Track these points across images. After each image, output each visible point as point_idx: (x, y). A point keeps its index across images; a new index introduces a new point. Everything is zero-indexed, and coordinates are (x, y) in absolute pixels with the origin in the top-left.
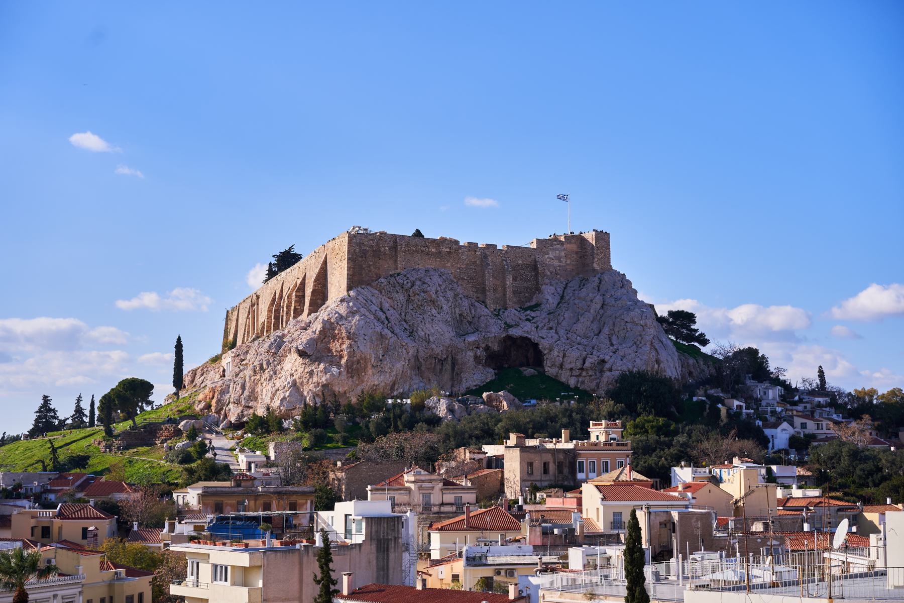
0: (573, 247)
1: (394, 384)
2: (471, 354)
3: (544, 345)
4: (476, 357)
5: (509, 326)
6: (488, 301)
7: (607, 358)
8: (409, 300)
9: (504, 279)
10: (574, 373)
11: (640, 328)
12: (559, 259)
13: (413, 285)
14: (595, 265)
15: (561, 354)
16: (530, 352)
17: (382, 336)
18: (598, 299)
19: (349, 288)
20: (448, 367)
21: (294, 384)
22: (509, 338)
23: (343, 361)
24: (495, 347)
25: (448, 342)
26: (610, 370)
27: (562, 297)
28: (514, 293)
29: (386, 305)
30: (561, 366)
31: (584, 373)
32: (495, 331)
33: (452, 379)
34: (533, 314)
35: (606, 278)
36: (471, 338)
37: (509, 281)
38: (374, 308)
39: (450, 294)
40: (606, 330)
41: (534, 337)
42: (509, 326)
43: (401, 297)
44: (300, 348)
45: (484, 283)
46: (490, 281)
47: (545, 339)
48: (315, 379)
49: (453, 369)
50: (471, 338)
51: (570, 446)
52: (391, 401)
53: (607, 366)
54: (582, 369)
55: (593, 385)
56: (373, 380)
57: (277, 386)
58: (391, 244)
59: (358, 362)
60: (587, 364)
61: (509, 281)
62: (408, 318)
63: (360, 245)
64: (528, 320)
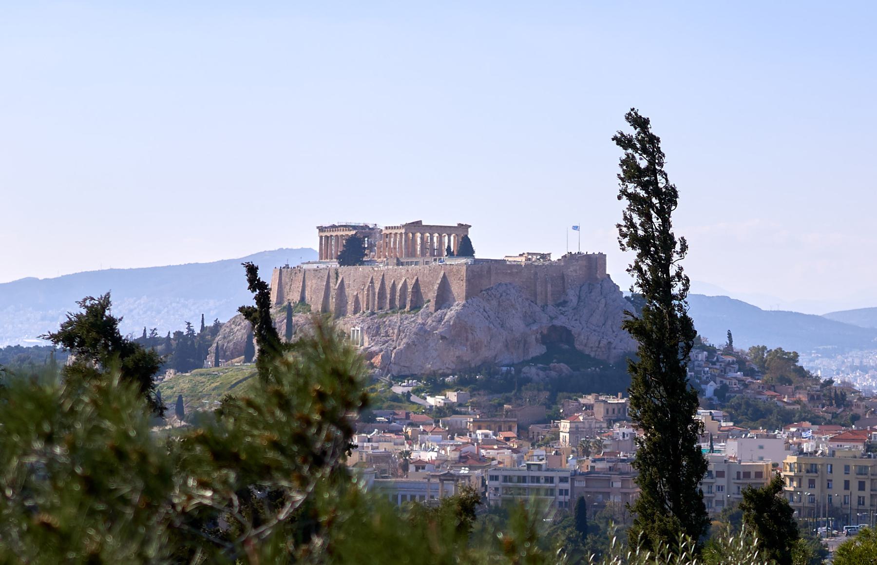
0: (584, 263)
1: (496, 355)
2: (534, 337)
3: (574, 331)
4: (536, 339)
5: (552, 318)
7: (612, 341)
8: (499, 305)
9: (546, 287)
12: (575, 271)
16: (566, 335)
17: (489, 329)
18: (603, 301)
19: (467, 298)
20: (522, 345)
22: (553, 326)
24: (545, 332)
27: (579, 297)
29: (487, 309)
30: (586, 345)
32: (545, 322)
34: (564, 309)
35: (605, 285)
36: (534, 328)
37: (549, 288)
38: (482, 310)
39: (520, 299)
40: (609, 323)
43: (494, 303)
46: (539, 289)
47: (575, 328)
50: (534, 328)
51: (623, 401)
53: (613, 346)
56: (486, 353)
60: (601, 345)
61: (549, 288)
62: (500, 315)
64: (562, 314)
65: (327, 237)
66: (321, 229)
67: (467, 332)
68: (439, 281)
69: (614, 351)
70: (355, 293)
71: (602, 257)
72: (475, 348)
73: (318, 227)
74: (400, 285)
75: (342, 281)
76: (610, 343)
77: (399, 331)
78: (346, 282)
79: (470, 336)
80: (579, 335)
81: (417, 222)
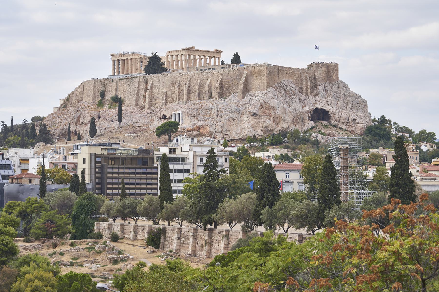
1: (289, 127)
2: (307, 115)
6: (304, 93)
7: (356, 118)
10: (345, 124)
11: (363, 106)
13: (287, 87)
14: (334, 77)
15: (339, 116)
21: (251, 126)
22: (317, 109)
23: (272, 118)
25: (301, 111)
26: (358, 123)
28: (311, 89)
30: (339, 121)
31: (348, 124)
33: (302, 125)
34: (318, 99)
41: (327, 108)
42: (314, 104)
43: (283, 92)
44: (255, 112)
45: (302, 85)
46: (304, 85)
47: (330, 109)
48: (261, 125)
49: (302, 121)
50: (307, 109)
52: (302, 134)
53: (357, 121)
54: (347, 122)
55: (353, 129)
57: (243, 126)
58: (277, 70)
59: (277, 118)
60: (350, 121)
63: (270, 71)
65: (119, 60)
66: (113, 56)
67: (270, 111)
68: (243, 78)
69: (359, 125)
70: (165, 91)
71: (336, 65)
72: (277, 121)
73: (111, 54)
74: (208, 83)
75: (152, 84)
76: (354, 120)
77: (218, 111)
78: (156, 84)
79: (272, 112)
80: (334, 114)
81: (192, 47)
